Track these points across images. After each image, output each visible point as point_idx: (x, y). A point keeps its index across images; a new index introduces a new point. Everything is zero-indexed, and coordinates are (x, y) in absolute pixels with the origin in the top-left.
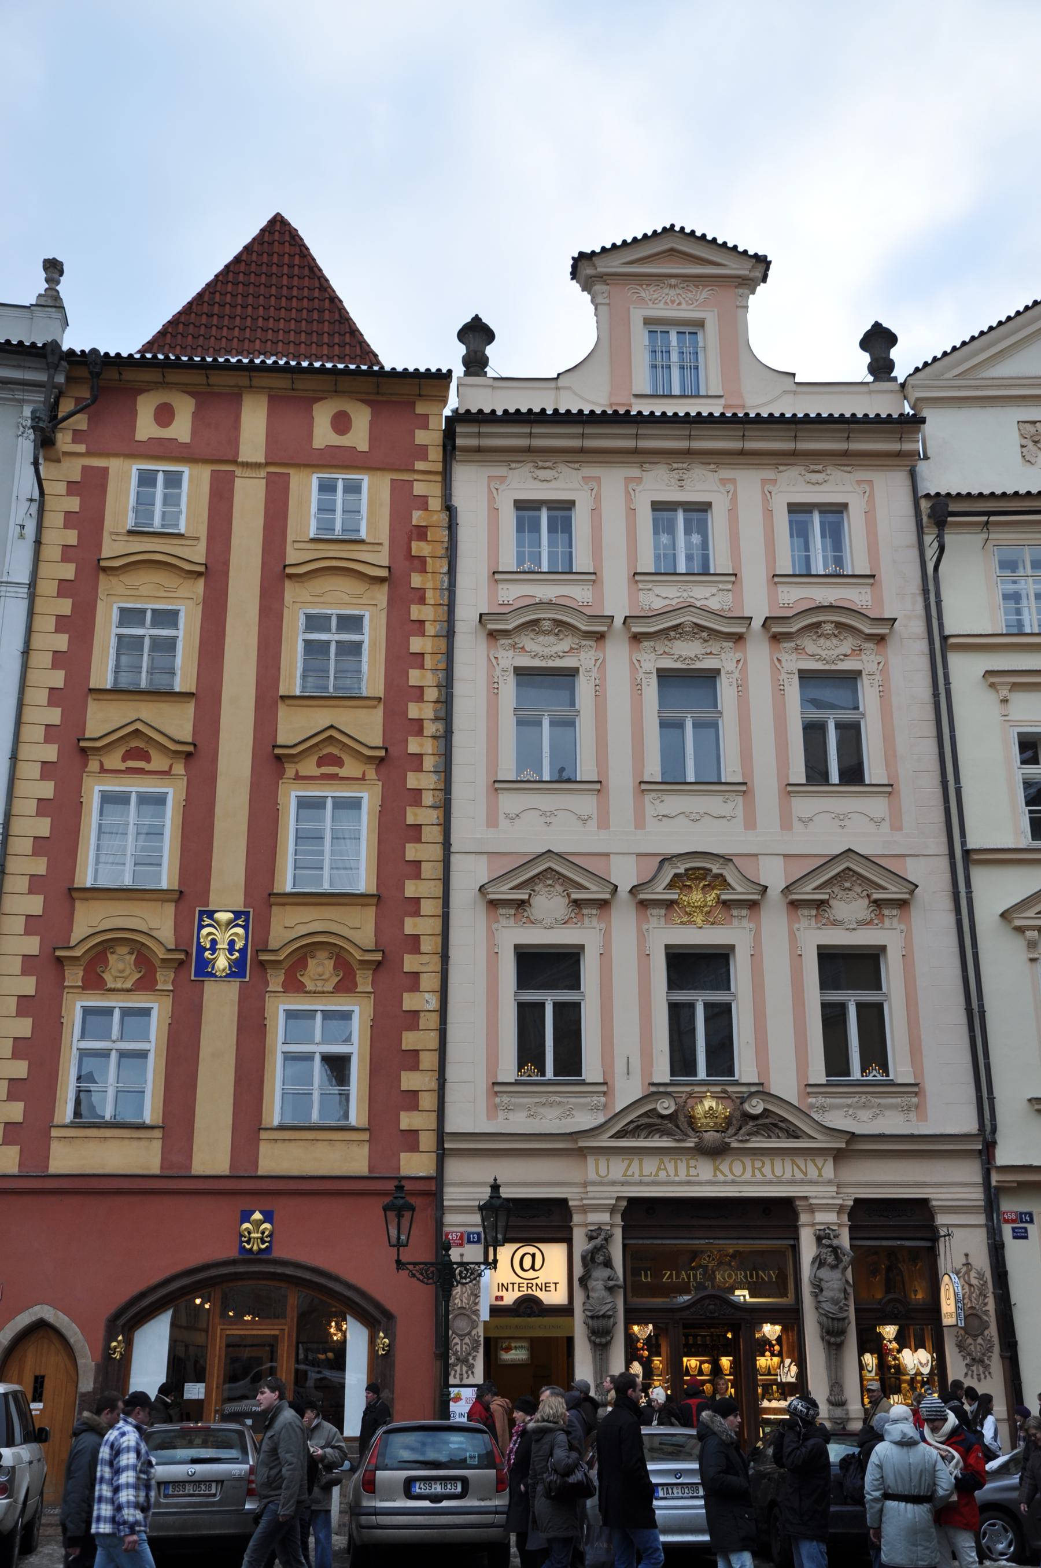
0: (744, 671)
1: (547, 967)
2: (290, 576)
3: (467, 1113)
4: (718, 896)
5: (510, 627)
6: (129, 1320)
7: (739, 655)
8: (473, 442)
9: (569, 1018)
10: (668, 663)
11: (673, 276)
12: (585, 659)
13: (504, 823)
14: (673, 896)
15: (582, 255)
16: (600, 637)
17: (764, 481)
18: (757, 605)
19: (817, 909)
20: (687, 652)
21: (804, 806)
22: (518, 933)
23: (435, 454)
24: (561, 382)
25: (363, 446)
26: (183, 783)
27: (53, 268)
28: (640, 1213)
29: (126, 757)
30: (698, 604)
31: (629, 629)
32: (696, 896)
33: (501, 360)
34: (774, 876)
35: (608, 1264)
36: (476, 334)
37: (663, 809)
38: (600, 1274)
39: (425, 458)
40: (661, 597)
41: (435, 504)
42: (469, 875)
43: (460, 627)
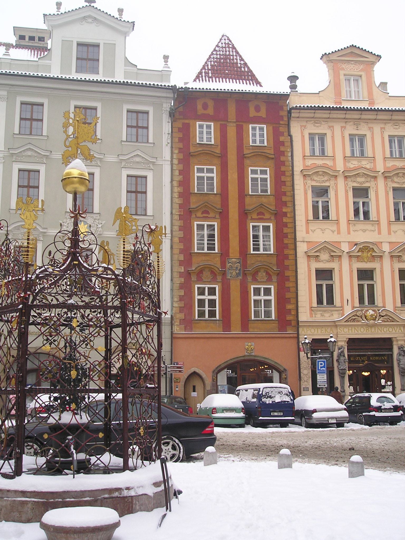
0: (377, 187)
1: (324, 274)
2: (245, 157)
3: (304, 316)
4: (371, 254)
5: (310, 173)
6: (219, 370)
7: (376, 182)
8: (297, 115)
9: (330, 289)
10: (355, 184)
11: (352, 60)
12: (331, 183)
13: (310, 232)
14: (360, 254)
15: (325, 54)
16: (336, 177)
17: (381, 128)
18: (380, 167)
19: (399, 257)
20: (360, 182)
21: (395, 227)
22: (316, 265)
23: (286, 119)
24: (320, 95)
25: (264, 116)
26: (219, 220)
27: (166, 58)
28: (352, 342)
29: (203, 213)
30: (364, 166)
31: (344, 174)
32: (365, 254)
33: (301, 87)
34: (386, 248)
35: (344, 356)
36: (293, 79)
37: (355, 228)
38: (342, 358)
39: (283, 120)
40: (353, 164)
41: (286, 134)
42: (302, 248)
43: (295, 173)
